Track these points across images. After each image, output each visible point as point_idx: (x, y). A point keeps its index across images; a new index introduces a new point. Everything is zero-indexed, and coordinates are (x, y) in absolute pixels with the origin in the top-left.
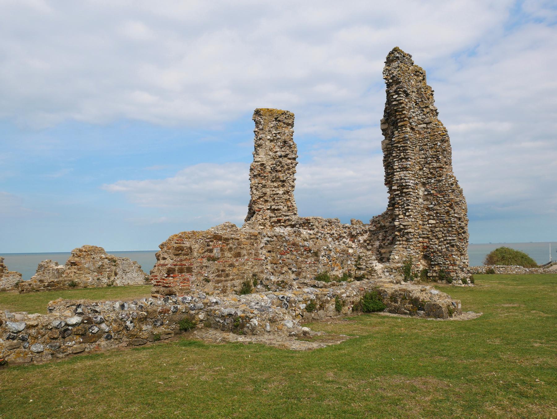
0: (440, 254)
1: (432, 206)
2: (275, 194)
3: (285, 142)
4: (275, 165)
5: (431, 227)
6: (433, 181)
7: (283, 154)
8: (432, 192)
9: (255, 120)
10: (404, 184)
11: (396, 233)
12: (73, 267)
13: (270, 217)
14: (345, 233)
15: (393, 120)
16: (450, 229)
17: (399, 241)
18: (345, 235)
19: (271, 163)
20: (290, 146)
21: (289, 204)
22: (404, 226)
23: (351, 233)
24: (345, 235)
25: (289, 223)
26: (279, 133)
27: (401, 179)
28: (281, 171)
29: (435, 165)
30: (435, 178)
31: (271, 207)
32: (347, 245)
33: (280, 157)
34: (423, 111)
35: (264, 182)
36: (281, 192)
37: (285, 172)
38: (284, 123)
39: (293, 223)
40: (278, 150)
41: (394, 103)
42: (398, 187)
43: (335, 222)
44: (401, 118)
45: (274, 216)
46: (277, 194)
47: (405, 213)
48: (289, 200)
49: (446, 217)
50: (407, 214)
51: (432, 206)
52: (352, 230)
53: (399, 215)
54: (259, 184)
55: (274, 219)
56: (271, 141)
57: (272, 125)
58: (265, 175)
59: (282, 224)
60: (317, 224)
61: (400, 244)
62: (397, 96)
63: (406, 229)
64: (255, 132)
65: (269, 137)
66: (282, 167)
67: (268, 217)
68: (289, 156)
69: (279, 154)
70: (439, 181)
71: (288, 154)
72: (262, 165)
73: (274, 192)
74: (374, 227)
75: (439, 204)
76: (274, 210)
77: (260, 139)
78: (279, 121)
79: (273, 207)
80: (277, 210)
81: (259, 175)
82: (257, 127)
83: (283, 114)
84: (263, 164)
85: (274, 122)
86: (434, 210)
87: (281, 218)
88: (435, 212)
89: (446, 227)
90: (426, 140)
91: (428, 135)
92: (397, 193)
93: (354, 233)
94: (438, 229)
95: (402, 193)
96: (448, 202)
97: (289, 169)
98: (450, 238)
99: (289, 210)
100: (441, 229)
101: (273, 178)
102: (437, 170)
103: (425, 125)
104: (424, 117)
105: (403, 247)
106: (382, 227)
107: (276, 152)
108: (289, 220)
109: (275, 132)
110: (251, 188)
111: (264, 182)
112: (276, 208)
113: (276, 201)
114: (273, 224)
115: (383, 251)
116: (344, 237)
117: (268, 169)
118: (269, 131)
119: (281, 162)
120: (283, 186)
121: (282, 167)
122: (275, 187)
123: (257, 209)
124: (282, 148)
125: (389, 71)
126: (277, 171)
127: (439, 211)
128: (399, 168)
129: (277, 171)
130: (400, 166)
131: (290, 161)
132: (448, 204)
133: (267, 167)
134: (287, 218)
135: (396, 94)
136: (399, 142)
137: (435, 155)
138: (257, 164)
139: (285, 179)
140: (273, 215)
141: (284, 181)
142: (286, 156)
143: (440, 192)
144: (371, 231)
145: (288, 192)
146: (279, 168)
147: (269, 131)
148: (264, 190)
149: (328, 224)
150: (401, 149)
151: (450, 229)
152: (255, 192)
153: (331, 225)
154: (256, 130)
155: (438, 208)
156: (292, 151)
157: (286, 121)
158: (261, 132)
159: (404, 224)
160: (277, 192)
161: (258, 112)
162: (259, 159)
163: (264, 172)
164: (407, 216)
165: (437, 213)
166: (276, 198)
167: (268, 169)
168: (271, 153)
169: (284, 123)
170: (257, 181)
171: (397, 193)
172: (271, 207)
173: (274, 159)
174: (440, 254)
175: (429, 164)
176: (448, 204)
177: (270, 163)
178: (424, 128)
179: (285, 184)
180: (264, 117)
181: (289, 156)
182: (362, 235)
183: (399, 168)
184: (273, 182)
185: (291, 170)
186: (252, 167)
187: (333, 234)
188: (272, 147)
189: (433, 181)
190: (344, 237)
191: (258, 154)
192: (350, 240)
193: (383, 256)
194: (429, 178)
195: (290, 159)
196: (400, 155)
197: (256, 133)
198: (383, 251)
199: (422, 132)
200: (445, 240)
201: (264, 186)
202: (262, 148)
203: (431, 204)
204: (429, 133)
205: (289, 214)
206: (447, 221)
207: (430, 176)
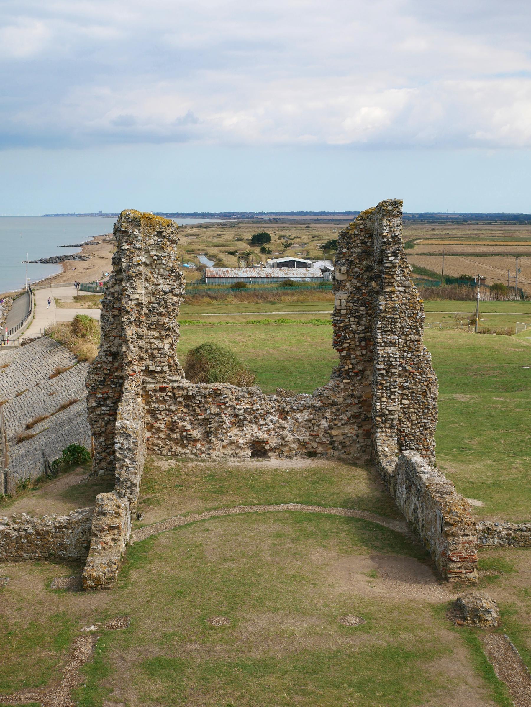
0: (413, 439)
1: (406, 384)
2: (154, 349)
4: (156, 305)
5: (404, 408)
6: (409, 356)
8: (408, 368)
10: (393, 363)
11: (378, 419)
12: (111, 532)
13: (143, 382)
14: (273, 408)
15: (356, 273)
16: (426, 411)
17: (382, 428)
18: (272, 411)
22: (388, 411)
23: (284, 409)
24: (272, 411)
27: (390, 357)
29: (413, 337)
30: (412, 352)
31: (147, 367)
32: (277, 425)
34: (403, 271)
39: (190, 393)
41: (387, 265)
42: (385, 365)
44: (389, 282)
45: (152, 381)
47: (390, 397)
49: (421, 397)
50: (393, 397)
51: (406, 384)
52: (284, 404)
53: (383, 397)
55: (153, 385)
57: (152, 242)
59: (169, 394)
60: (230, 395)
61: (383, 432)
62: (393, 258)
63: (389, 414)
67: (141, 382)
70: (417, 356)
73: (154, 346)
74: (320, 403)
75: (416, 382)
76: (155, 371)
78: (165, 237)
79: (152, 368)
85: (156, 238)
86: (408, 389)
87: (165, 385)
88: (410, 391)
89: (421, 408)
90: (404, 307)
91: (408, 301)
92: (382, 372)
93: (287, 409)
94: (412, 410)
95: (387, 372)
96: (426, 381)
98: (425, 421)
100: (416, 411)
101: (152, 325)
102: (416, 343)
103: (403, 289)
104: (404, 278)
105: (387, 436)
106: (334, 404)
107: (159, 285)
112: (158, 369)
114: (150, 393)
115: (334, 432)
116: (271, 413)
117: (145, 310)
119: (166, 302)
123: (131, 373)
125: (390, 227)
127: (415, 391)
128: (384, 342)
129: (161, 314)
130: (385, 340)
132: (426, 384)
134: (176, 384)
135: (393, 256)
136: (385, 311)
137: (414, 326)
140: (149, 379)
143: (417, 369)
144: (315, 407)
146: (162, 310)
148: (142, 343)
149: (247, 395)
150: (390, 320)
151: (426, 411)
153: (251, 397)
155: (414, 387)
159: (390, 408)
160: (161, 346)
162: (137, 297)
164: (392, 400)
165: (413, 392)
166: (158, 355)
167: (145, 310)
168: (147, 285)
169: (169, 240)
171: (382, 372)
172: (147, 367)
173: (153, 294)
174: (413, 439)
175: (407, 335)
176: (426, 384)
178: (402, 291)
179: (170, 334)
182: (301, 411)
183: (384, 342)
184: (149, 328)
187: (258, 409)
189: (409, 356)
190: (271, 413)
191: (135, 288)
192: (279, 417)
193: (334, 439)
194: (404, 351)
196: (387, 327)
198: (334, 432)
199: (400, 297)
200: (419, 423)
201: (140, 337)
203: (407, 382)
204: (409, 299)
206: (423, 402)
207: (406, 349)
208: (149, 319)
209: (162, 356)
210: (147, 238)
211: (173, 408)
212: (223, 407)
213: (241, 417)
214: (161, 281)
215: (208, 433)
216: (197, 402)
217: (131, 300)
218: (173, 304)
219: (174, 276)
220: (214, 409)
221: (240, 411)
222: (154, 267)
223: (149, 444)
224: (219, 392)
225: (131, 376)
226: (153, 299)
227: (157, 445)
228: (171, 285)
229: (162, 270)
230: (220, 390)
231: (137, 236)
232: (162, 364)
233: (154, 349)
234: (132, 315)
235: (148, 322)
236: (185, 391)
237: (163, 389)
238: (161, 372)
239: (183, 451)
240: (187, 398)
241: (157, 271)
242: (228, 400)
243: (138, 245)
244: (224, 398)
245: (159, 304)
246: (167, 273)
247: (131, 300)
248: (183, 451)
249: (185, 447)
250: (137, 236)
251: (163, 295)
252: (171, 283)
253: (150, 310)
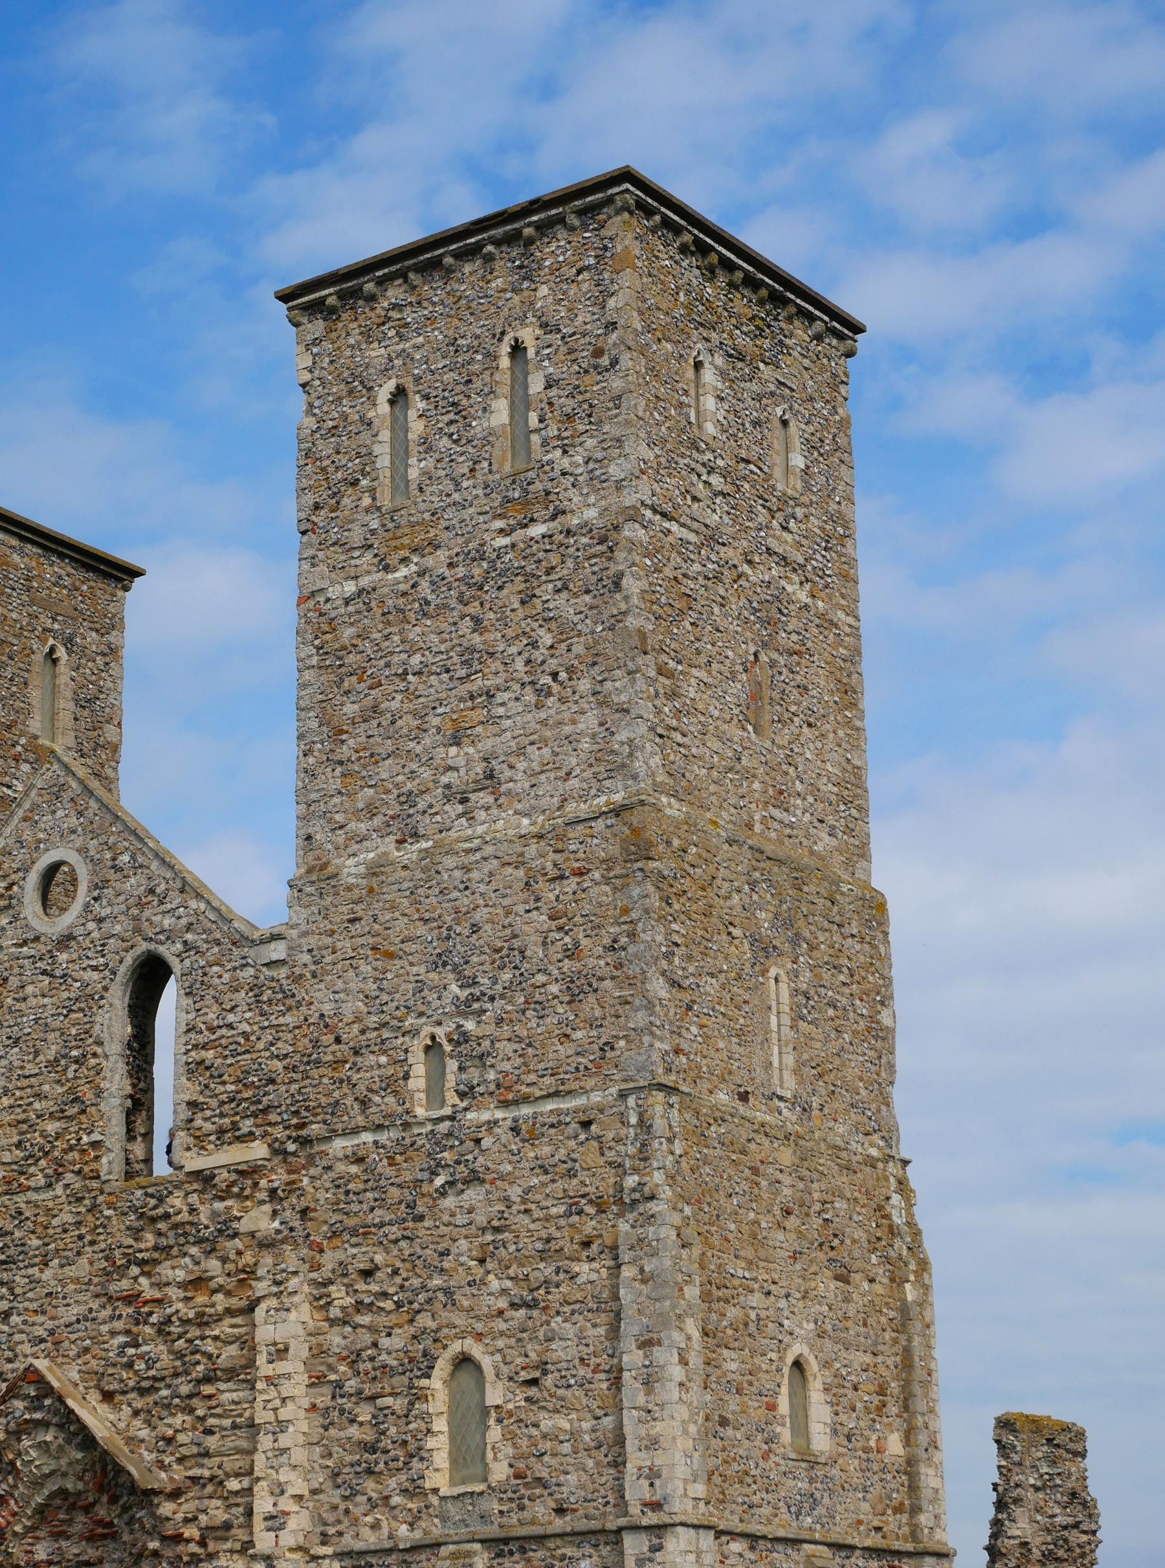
3: (1074, 1495)
4: (1052, 1547)
7: (1070, 1520)
9: (998, 1442)
19: (1040, 1539)
20: (1084, 1504)
26: (1059, 1474)
28: (1066, 1560)
33: (1065, 1528)
37: (1075, 1562)
56: (1037, 1489)
57: (1040, 1455)
64: (999, 1467)
65: (1032, 1481)
66: (1069, 1550)
68: (1084, 1527)
71: (1080, 1522)
72: (1024, 1544)
78: (1058, 1446)
82: (1006, 1457)
83: (1064, 1430)
84: (1027, 1543)
85: (1045, 1448)
97: (1083, 1555)
107: (1054, 1516)
109: (1046, 1470)
117: (1036, 1554)
118: (1033, 1467)
119: (1066, 1540)
121: (1069, 1550)
126: (1057, 1559)
129: (1057, 1559)
131: (1084, 1538)
133: (1034, 1550)
138: (1012, 1542)
142: (1076, 1525)
146: (1061, 1553)
154: (1003, 1463)
156: (1090, 1516)
157: (1071, 1446)
158: (1016, 1469)
161: (1005, 1424)
162: (1018, 1533)
167: (1036, 1554)
168: (1039, 1518)
169: (1068, 1451)
173: (1048, 1531)
177: (1039, 1540)
180: (1022, 1436)
181: (1084, 1527)
185: (1089, 1558)
188: (1042, 1503)
191: (1014, 1521)
195: (1084, 1532)
202: (1021, 1506)
210: (1034, 1449)
214: (1057, 1511)
217: (1009, 1538)
218: (1078, 1545)
226: (1049, 1539)
228: (1075, 1516)
229: (1059, 1496)
231: (1015, 1447)
243: (1016, 1458)
245: (1055, 1545)
246: (1066, 1499)
247: (1009, 1538)
250: (1015, 1447)
252: (1075, 1513)
253: (1044, 1555)
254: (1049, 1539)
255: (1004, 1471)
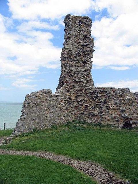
2: (78, 71)
3: (86, 36)
19: (76, 50)
20: (89, 39)
21: (88, 79)
25: (89, 91)
26: (82, 30)
28: (83, 55)
31: (75, 80)
33: (83, 45)
35: (71, 63)
36: (83, 70)
38: (85, 24)
39: (92, 91)
40: (81, 41)
43: (127, 91)
46: (80, 71)
48: (88, 76)
54: (67, 64)
57: (77, 26)
58: (71, 58)
59: (84, 92)
64: (65, 30)
65: (74, 34)
69: (81, 44)
71: (88, 44)
76: (77, 82)
77: (69, 34)
78: (82, 22)
79: (77, 80)
80: (79, 82)
81: (68, 58)
84: (71, 51)
87: (82, 88)
97: (88, 54)
99: (88, 83)
108: (89, 89)
110: (62, 66)
111: (71, 63)
112: (79, 81)
113: (79, 76)
117: (74, 54)
119: (83, 49)
120: (84, 66)
121: (83, 53)
122: (79, 66)
124: (84, 40)
126: (80, 55)
129: (80, 55)
133: (73, 53)
139: (85, 61)
141: (85, 62)
142: (86, 46)
145: (88, 70)
146: (81, 53)
147: (75, 30)
148: (71, 68)
152: (64, 69)
156: (91, 43)
161: (68, 17)
162: (68, 47)
163: (71, 56)
167: (74, 54)
169: (85, 24)
170: (66, 62)
172: (75, 80)
173: (78, 47)
177: (75, 50)
186: (63, 52)
195: (89, 47)
197: (66, 31)
201: (71, 66)
205: (88, 85)
208: (76, 58)
209: (81, 74)
210: (75, 25)
211: (86, 99)
212: (107, 98)
213: (118, 104)
215: (101, 112)
216: (95, 96)
219: (88, 39)
220: (103, 100)
221: (117, 101)
222: (79, 36)
223: (76, 116)
224: (105, 90)
225: (65, 83)
227: (79, 117)
230: (106, 89)
232: (81, 78)
233: (78, 71)
234: (64, 55)
235: (76, 60)
236: (91, 90)
237: (81, 90)
238: (81, 82)
239: (89, 121)
240: (92, 94)
241: (80, 38)
242: (110, 95)
243: (70, 27)
244: (108, 93)
246: (84, 37)
248: (89, 121)
249: (91, 119)
251: (81, 47)
253: (76, 55)
254: (78, 50)
255: (66, 31)
